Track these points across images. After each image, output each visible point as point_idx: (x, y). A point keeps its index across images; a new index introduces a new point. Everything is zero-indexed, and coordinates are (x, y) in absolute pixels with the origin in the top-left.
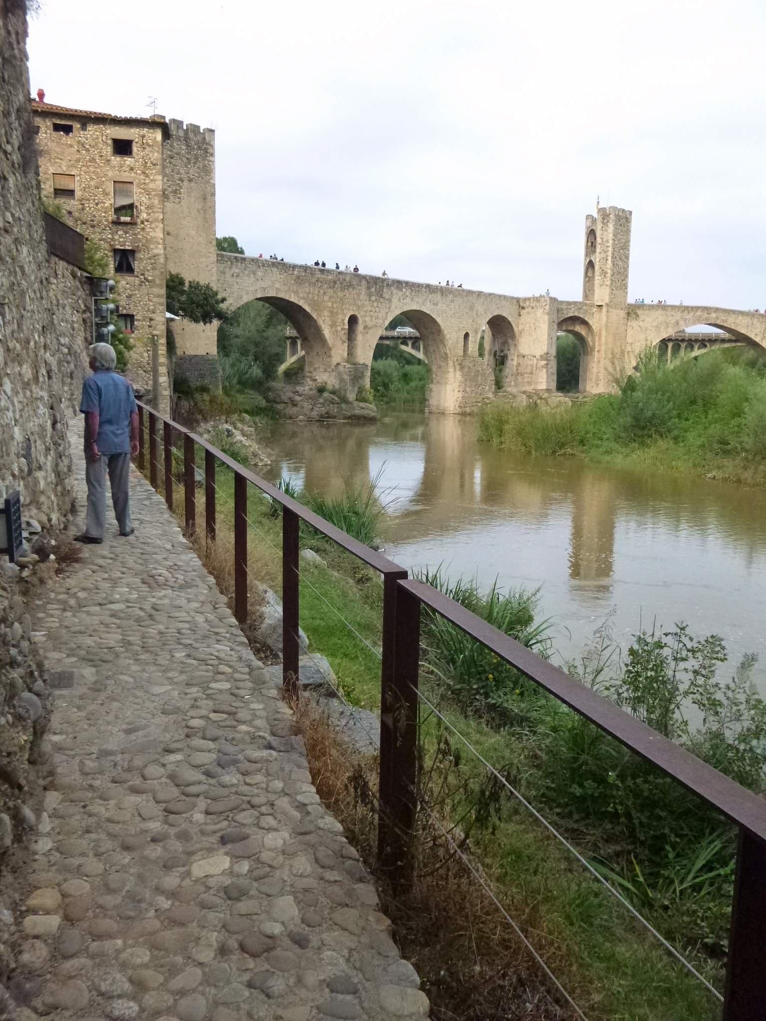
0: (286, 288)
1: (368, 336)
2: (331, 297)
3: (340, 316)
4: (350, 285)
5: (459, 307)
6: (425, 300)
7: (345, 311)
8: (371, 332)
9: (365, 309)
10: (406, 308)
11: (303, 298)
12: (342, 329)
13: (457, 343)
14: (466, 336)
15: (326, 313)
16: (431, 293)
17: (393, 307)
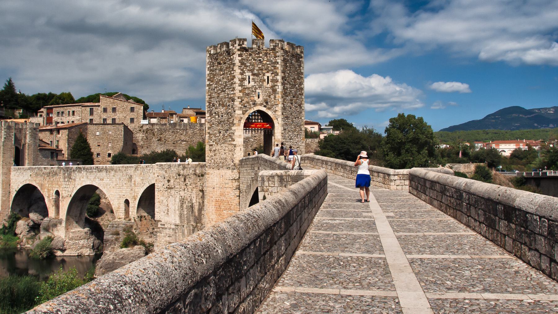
0: (32, 179)
1: (64, 202)
2: (48, 181)
3: (51, 191)
4: (56, 174)
5: (120, 179)
6: (95, 178)
7: (54, 188)
8: (65, 200)
9: (62, 186)
10: (84, 184)
11: (38, 183)
12: (52, 198)
13: (119, 208)
14: (127, 202)
15: (46, 190)
16: (99, 172)
17: (76, 184)
